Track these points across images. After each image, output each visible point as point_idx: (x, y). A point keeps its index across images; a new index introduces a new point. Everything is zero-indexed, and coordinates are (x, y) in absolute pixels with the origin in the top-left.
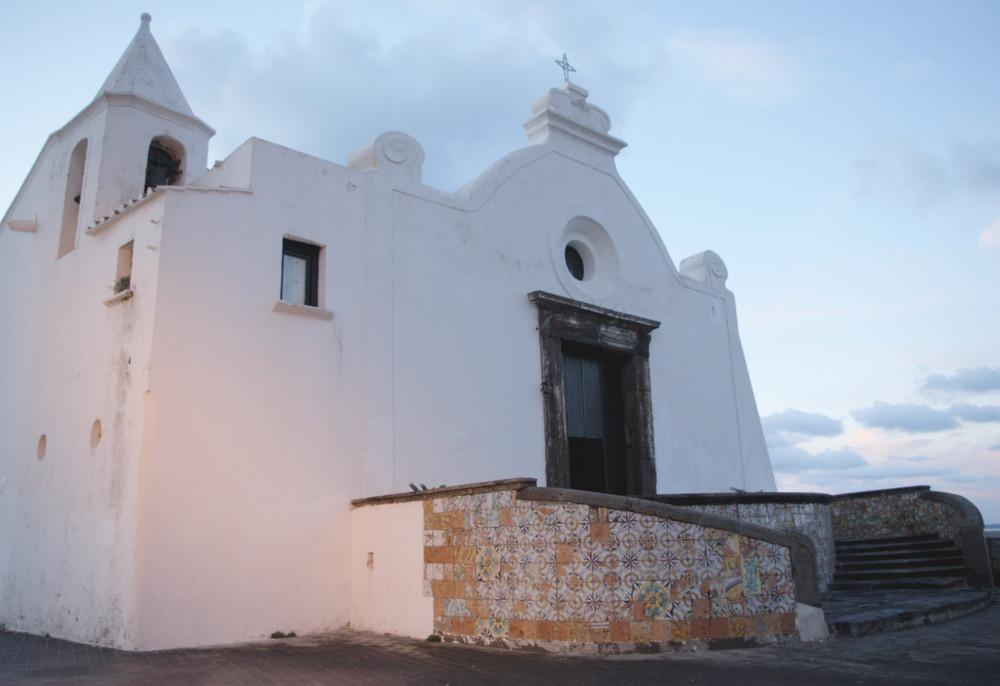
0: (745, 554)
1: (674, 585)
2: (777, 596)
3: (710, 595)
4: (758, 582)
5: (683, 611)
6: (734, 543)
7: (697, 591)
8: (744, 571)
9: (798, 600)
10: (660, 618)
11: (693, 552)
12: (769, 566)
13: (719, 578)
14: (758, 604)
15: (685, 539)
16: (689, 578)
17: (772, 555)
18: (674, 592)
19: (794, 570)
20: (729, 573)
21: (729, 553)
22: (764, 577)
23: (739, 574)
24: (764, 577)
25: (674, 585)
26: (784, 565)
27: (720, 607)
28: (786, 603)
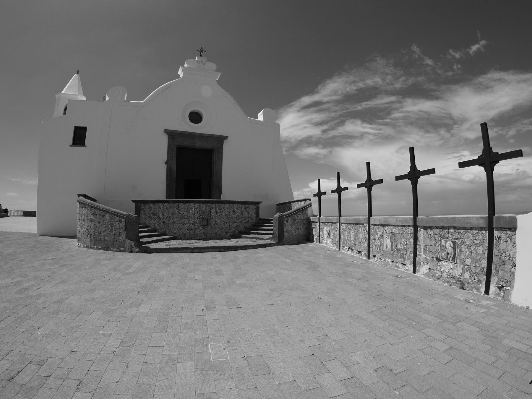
17: (120, 222)
19: (126, 227)
28: (123, 237)
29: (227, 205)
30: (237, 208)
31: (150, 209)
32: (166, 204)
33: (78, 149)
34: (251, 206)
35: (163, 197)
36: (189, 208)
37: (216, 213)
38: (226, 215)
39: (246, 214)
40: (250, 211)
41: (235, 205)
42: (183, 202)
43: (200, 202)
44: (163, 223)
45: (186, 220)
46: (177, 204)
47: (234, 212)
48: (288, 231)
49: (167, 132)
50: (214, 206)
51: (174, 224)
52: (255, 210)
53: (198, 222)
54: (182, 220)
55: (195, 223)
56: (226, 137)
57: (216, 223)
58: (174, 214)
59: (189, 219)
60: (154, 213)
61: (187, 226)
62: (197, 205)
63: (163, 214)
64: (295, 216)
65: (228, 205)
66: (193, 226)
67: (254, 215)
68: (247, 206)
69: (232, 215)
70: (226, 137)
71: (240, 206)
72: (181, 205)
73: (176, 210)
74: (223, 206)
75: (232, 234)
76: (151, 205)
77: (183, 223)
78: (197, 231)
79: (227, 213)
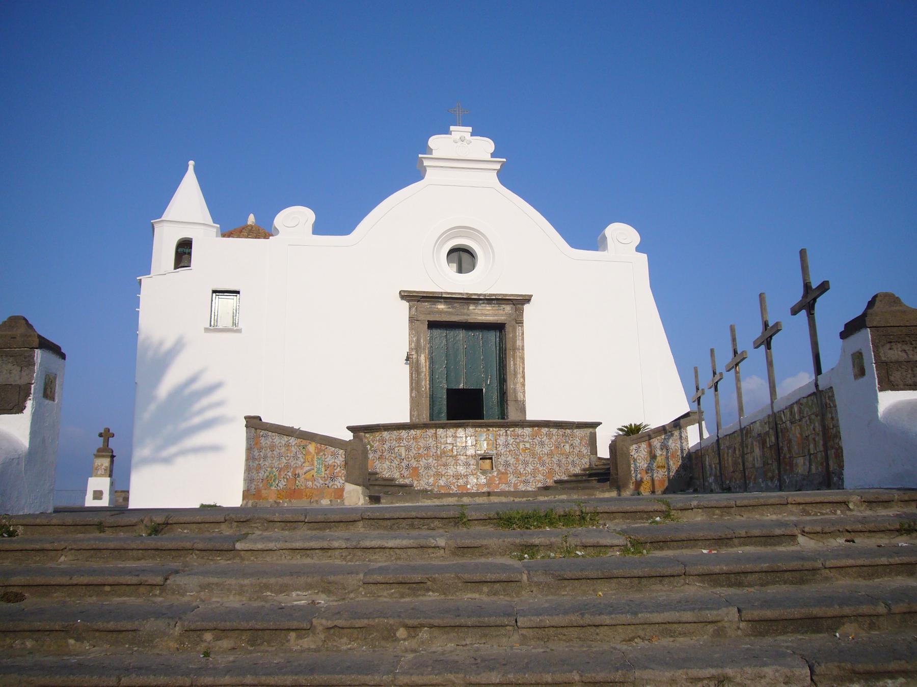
0: (317, 454)
1: (280, 470)
2: (333, 479)
3: (296, 476)
4: (323, 470)
5: (282, 484)
6: (312, 448)
7: (290, 474)
8: (316, 463)
9: (346, 481)
10: (273, 488)
11: (291, 452)
12: (330, 460)
13: (302, 467)
14: (321, 482)
15: (288, 445)
16: (288, 466)
17: (334, 455)
18: (280, 474)
19: (346, 464)
20: (307, 464)
21: (309, 453)
22: (327, 467)
23: (313, 465)
24: (327, 467)
25: (280, 470)
26: (340, 460)
27: (300, 482)
30: (549, 436)
31: (383, 441)
32: (413, 432)
34: (577, 432)
35: (405, 419)
37: (506, 445)
38: (527, 449)
39: (567, 447)
40: (577, 442)
41: (544, 430)
43: (474, 426)
44: (408, 467)
46: (433, 431)
47: (542, 444)
49: (407, 296)
50: (502, 431)
51: (428, 467)
53: (472, 462)
54: (444, 460)
56: (527, 299)
57: (507, 464)
58: (428, 448)
60: (391, 449)
61: (451, 471)
63: (408, 449)
65: (530, 429)
67: (585, 451)
68: (568, 431)
69: (538, 449)
70: (527, 299)
71: (554, 431)
72: (440, 431)
73: (431, 442)
74: (519, 431)
75: (540, 485)
76: (385, 434)
79: (528, 445)
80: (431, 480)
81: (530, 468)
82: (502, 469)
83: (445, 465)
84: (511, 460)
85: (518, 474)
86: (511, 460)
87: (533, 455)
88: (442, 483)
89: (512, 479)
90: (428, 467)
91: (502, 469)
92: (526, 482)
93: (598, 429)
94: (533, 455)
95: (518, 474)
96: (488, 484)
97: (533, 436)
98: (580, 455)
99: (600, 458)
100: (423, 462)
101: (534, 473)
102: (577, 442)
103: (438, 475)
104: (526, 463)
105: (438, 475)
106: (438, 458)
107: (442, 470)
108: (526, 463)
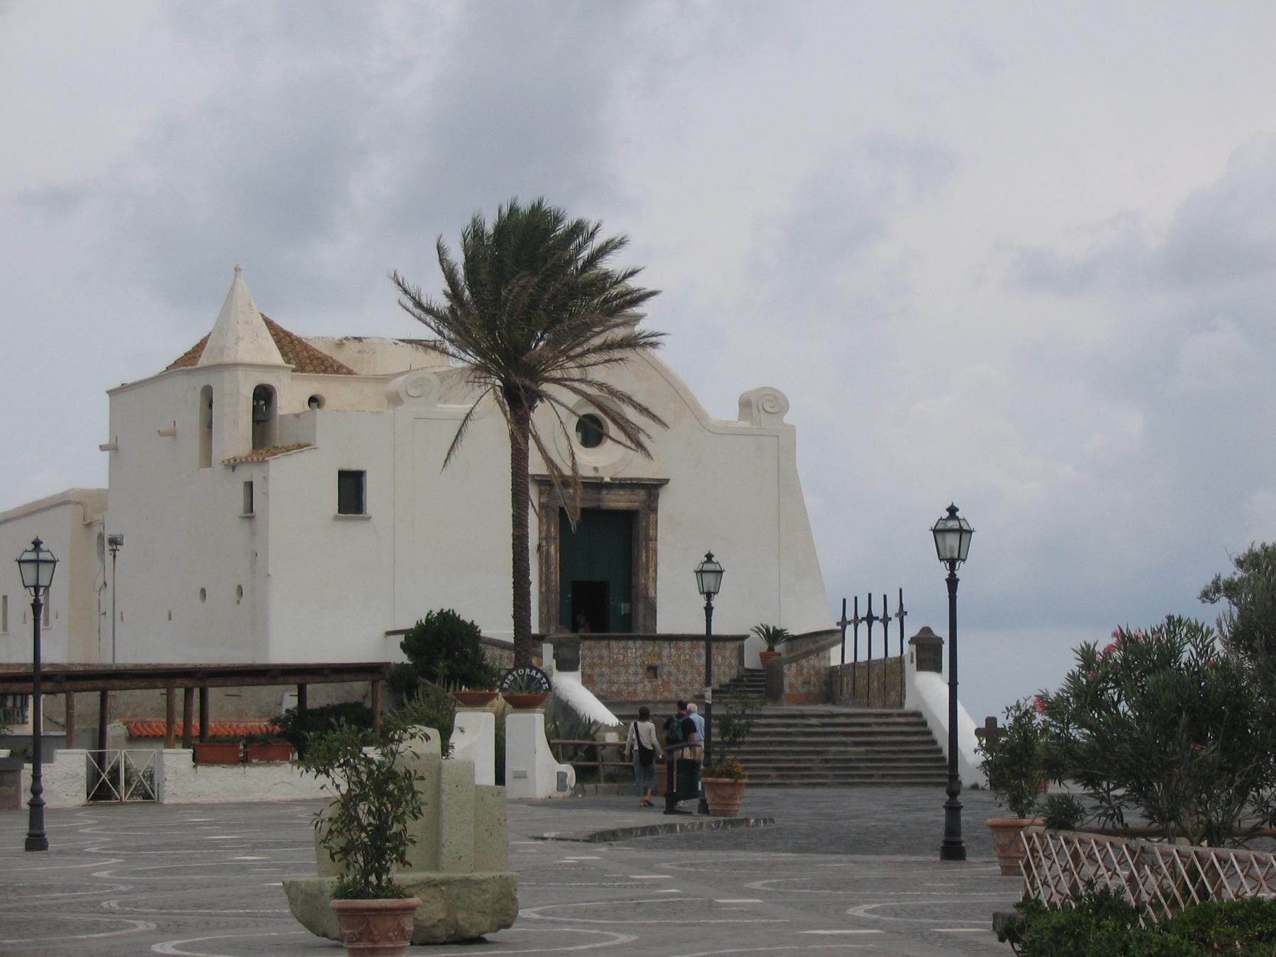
29: (687, 644)
33: (352, 528)
36: (626, 648)
37: (670, 657)
42: (616, 638)
45: (622, 670)
48: (791, 686)
50: (666, 644)
51: (602, 675)
52: (735, 653)
53: (640, 670)
55: (636, 674)
57: (670, 674)
58: (601, 658)
59: (627, 666)
61: (623, 678)
62: (639, 643)
64: (804, 662)
66: (632, 679)
67: (734, 662)
72: (613, 643)
73: (605, 653)
74: (681, 644)
77: (618, 673)
78: (640, 687)
80: (605, 687)
81: (688, 678)
82: (665, 678)
83: (618, 673)
84: (673, 670)
85: (678, 683)
86: (673, 670)
87: (692, 666)
88: (614, 689)
89: (674, 687)
90: (602, 675)
91: (665, 678)
92: (685, 691)
93: (746, 642)
94: (692, 666)
95: (678, 683)
96: (654, 691)
97: (692, 649)
98: (730, 666)
99: (746, 670)
100: (597, 670)
101: (691, 683)
102: (728, 653)
103: (611, 682)
104: (685, 673)
105: (611, 682)
106: (611, 667)
107: (615, 678)
108: (685, 673)
